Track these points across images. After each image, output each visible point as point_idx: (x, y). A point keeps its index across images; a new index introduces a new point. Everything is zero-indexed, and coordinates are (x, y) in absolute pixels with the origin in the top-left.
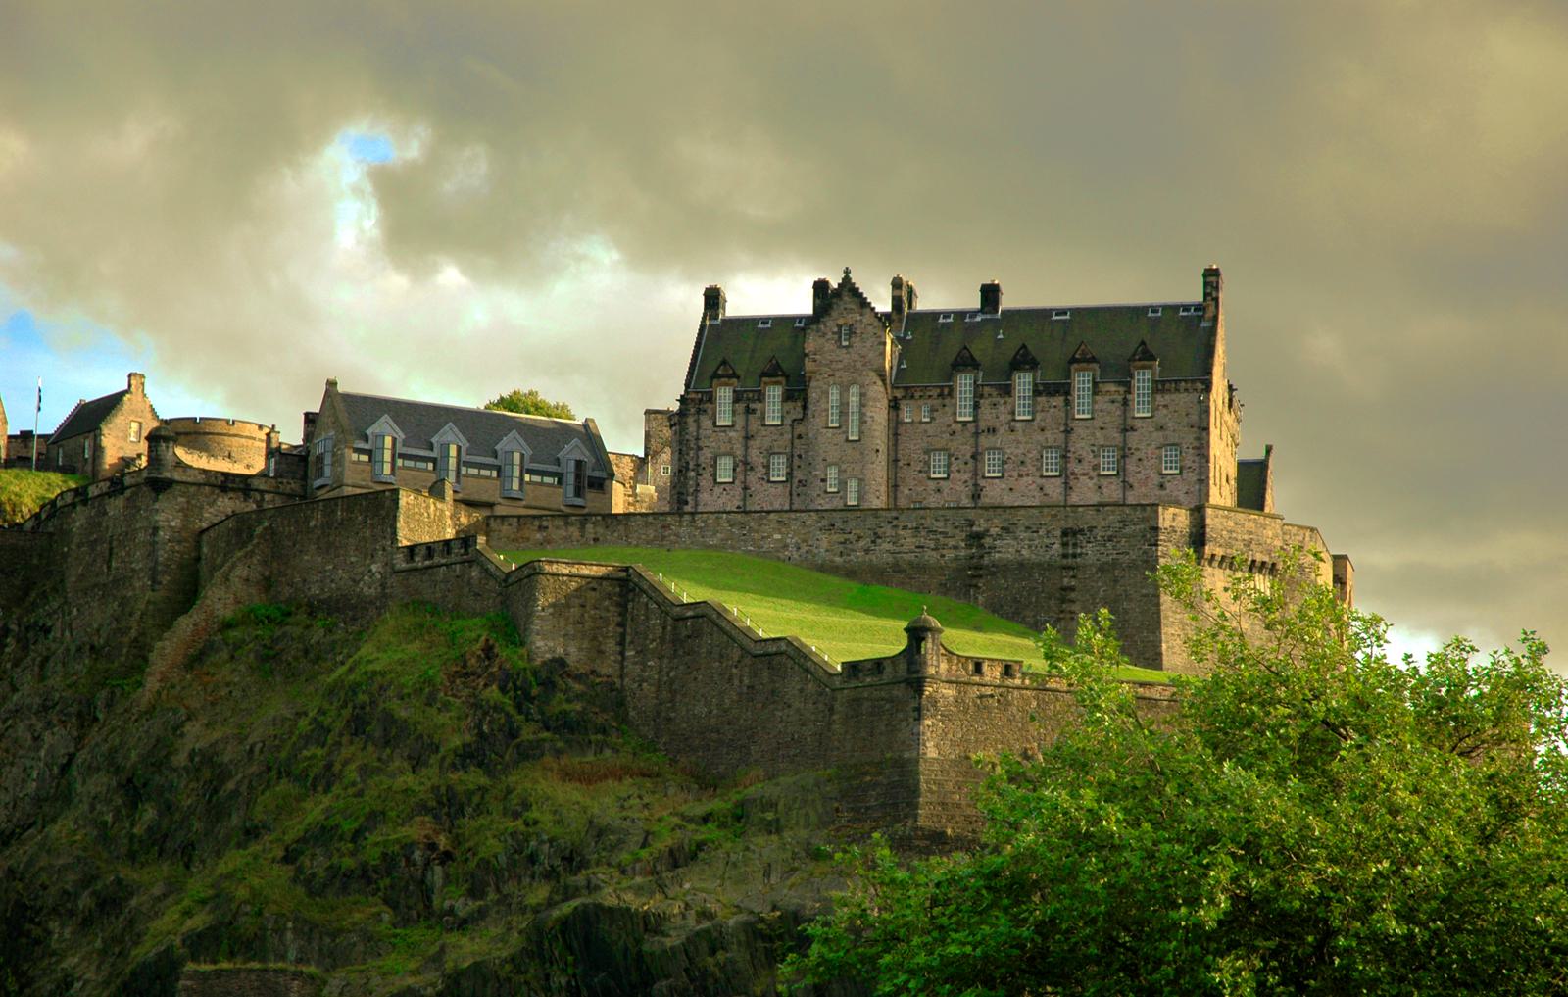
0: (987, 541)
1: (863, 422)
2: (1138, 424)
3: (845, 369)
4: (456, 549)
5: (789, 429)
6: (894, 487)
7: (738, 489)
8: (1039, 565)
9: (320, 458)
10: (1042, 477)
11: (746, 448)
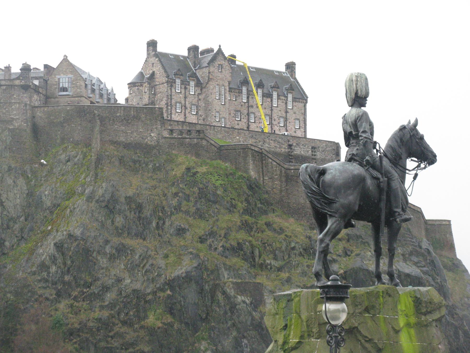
0: (293, 147)
1: (225, 99)
2: (289, 110)
3: (221, 79)
4: (194, 134)
5: (196, 96)
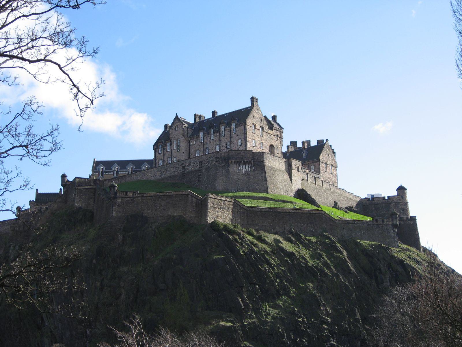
0: (186, 167)
2: (233, 135)
11: (164, 157)
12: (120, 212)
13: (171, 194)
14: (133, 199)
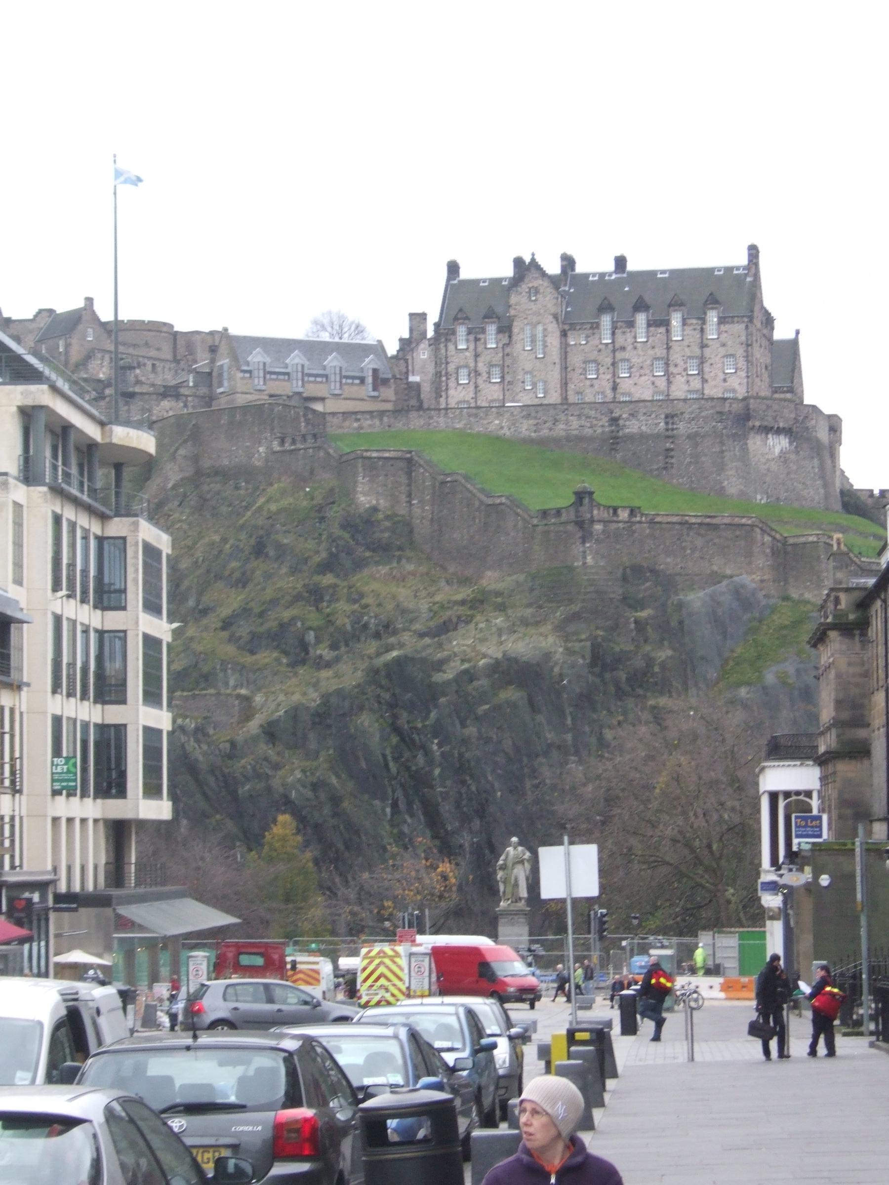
0: (621, 422)
1: (545, 346)
2: (710, 343)
5: (501, 350)
6: (565, 384)
7: (472, 388)
8: (652, 435)
9: (220, 375)
10: (654, 376)
11: (476, 362)
12: (603, 557)
13: (715, 521)
14: (631, 526)
